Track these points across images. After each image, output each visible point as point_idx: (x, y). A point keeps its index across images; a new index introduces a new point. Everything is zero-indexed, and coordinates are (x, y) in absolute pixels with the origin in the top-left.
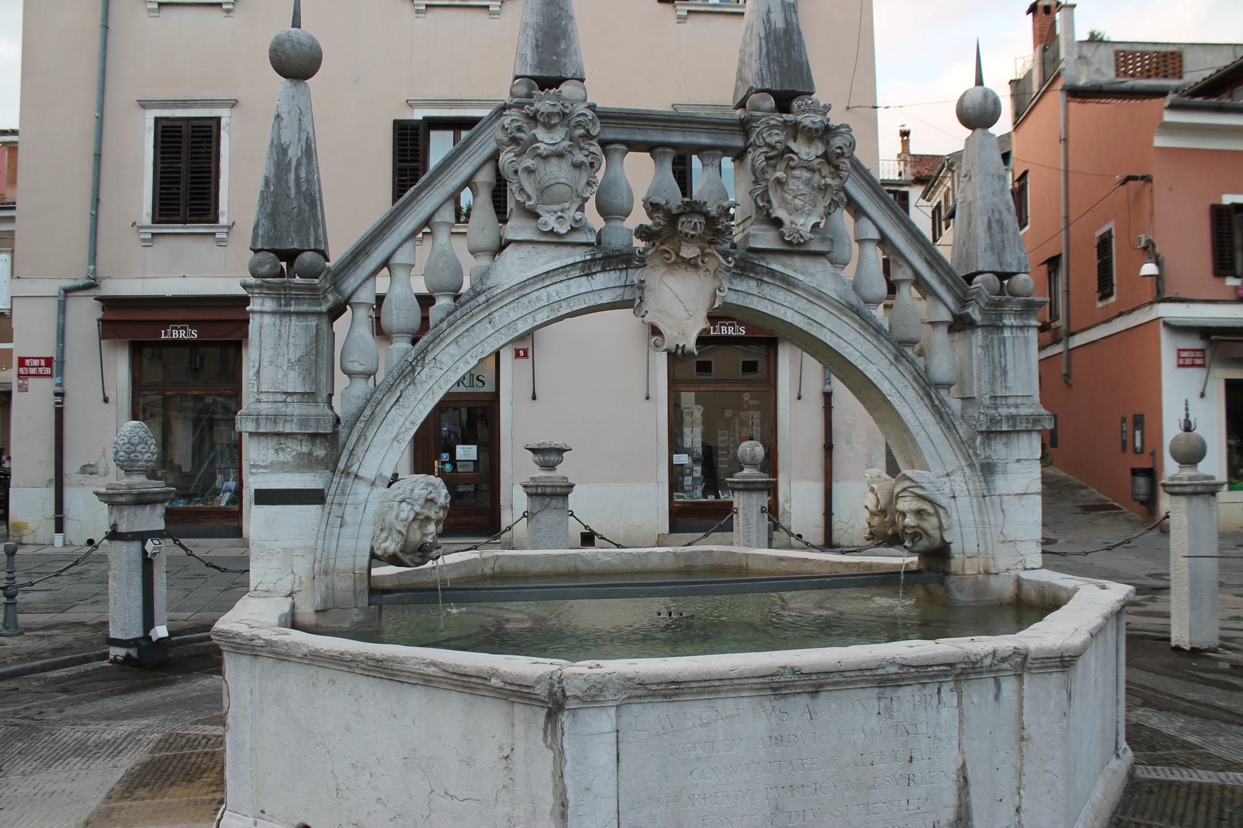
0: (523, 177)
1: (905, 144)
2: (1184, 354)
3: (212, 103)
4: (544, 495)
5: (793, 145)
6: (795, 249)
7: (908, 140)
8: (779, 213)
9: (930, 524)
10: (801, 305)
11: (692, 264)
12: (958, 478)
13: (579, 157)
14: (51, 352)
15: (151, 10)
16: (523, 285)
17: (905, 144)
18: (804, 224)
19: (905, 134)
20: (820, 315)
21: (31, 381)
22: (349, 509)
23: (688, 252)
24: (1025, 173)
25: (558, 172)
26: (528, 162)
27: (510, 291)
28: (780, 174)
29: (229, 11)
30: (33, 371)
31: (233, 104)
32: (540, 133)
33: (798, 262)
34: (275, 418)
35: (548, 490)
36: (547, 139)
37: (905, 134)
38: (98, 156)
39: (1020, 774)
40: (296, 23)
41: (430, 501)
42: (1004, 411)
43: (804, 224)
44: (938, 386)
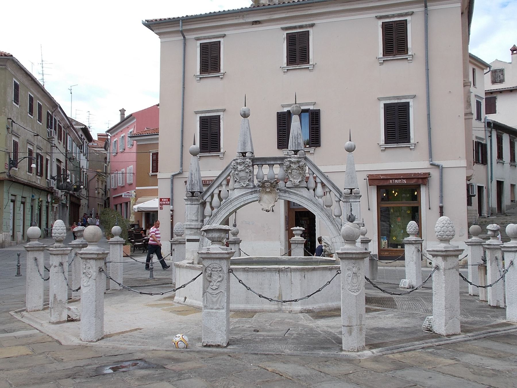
0: (236, 176)
3: (218, 111)
4: (295, 243)
5: (291, 165)
6: (296, 187)
9: (327, 249)
10: (299, 199)
11: (269, 192)
13: (247, 171)
14: (169, 197)
15: (197, 80)
16: (238, 197)
18: (297, 182)
20: (303, 201)
21: (164, 206)
23: (268, 190)
25: (242, 174)
26: (237, 172)
27: (235, 198)
29: (222, 78)
30: (164, 203)
31: (224, 111)
32: (238, 166)
33: (299, 189)
34: (190, 225)
35: (296, 242)
36: (240, 168)
38: (182, 131)
39: (291, 290)
43: (297, 182)
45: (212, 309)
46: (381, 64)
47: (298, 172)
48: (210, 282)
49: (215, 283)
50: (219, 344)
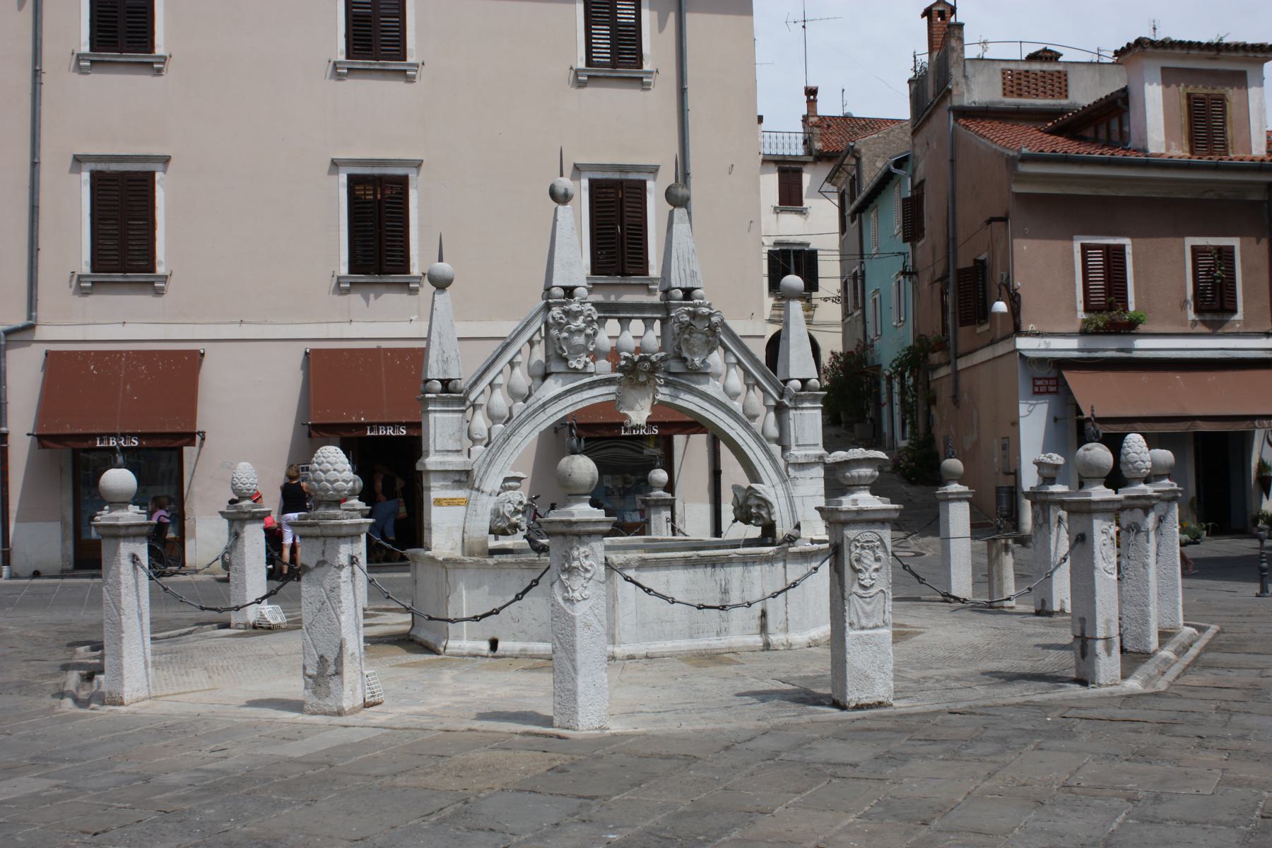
1: (812, 103)
2: (1039, 383)
7: (815, 101)
8: (686, 354)
9: (763, 513)
10: (696, 400)
11: (644, 384)
12: (779, 488)
13: (589, 331)
17: (812, 103)
19: (811, 93)
20: (706, 405)
22: (479, 508)
24: (922, 182)
26: (565, 335)
28: (686, 336)
33: (695, 378)
37: (811, 93)
40: (441, 260)
41: (521, 503)
42: (803, 453)
44: (768, 439)
45: (863, 628)
46: (581, 85)
47: (704, 338)
48: (860, 571)
49: (867, 575)
50: (881, 699)
